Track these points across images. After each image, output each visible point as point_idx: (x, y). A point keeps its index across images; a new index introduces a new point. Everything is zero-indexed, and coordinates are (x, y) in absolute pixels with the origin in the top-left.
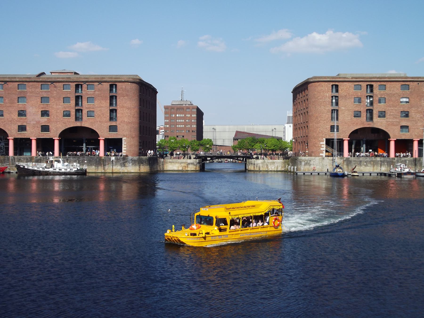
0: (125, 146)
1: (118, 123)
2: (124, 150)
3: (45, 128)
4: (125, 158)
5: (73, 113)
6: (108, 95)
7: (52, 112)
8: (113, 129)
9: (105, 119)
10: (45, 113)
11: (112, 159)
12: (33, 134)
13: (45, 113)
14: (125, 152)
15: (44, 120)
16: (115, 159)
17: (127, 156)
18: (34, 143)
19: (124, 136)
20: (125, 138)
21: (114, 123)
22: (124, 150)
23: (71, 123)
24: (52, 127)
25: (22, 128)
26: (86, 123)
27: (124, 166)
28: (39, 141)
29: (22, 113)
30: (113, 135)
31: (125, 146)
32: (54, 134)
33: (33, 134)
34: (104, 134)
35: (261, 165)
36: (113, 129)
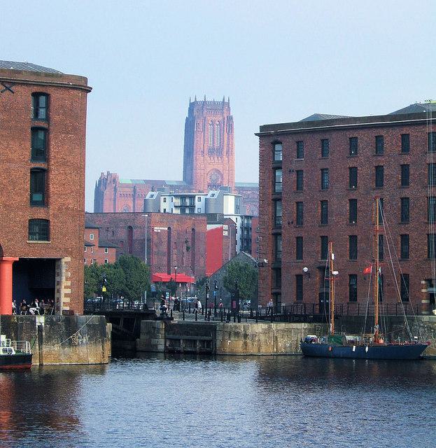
0: (69, 283)
1: (51, 212)
2: (66, 295)
4: (70, 325)
6: (26, 120)
9: (18, 199)
11: (38, 324)
14: (68, 300)
16: (46, 321)
17: (71, 312)
19: (70, 254)
20: (68, 259)
21: (40, 214)
22: (66, 295)
27: (71, 344)
30: (37, 250)
31: (69, 283)
35: (262, 338)
36: (41, 229)
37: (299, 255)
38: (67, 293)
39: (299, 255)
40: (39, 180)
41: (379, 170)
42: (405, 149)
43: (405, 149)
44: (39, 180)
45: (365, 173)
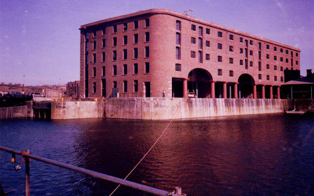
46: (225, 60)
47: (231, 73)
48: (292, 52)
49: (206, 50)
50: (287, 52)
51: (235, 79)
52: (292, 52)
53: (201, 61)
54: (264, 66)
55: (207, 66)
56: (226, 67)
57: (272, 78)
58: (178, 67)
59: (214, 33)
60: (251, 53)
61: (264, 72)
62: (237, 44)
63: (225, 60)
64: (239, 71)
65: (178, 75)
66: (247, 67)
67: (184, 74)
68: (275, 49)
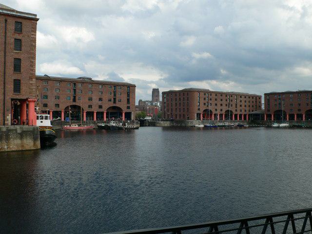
3: (100, 107)
4: (133, 122)
5: (112, 100)
7: (104, 99)
8: (128, 108)
10: (100, 99)
12: (95, 109)
13: (100, 99)
15: (100, 103)
18: (95, 114)
23: (111, 104)
24: (103, 107)
25: (90, 106)
26: (118, 105)
28: (97, 113)
29: (90, 99)
30: (128, 111)
32: (104, 110)
33: (95, 109)
34: (125, 110)
36: (128, 108)
37: (168, 111)
38: (133, 117)
39: (168, 111)
40: (128, 100)
41: (180, 98)
42: (184, 95)
43: (184, 95)
44: (128, 100)
45: (178, 99)
46: (219, 105)
47: (221, 110)
48: (256, 98)
49: (210, 102)
50: (253, 98)
51: (223, 112)
52: (256, 98)
53: (208, 106)
54: (238, 106)
55: (210, 108)
56: (219, 108)
57: (243, 111)
58: (199, 109)
59: (213, 95)
60: (232, 101)
61: (239, 108)
62: (224, 97)
63: (219, 105)
64: (225, 109)
65: (199, 112)
66: (229, 107)
67: (201, 112)
68: (245, 97)
